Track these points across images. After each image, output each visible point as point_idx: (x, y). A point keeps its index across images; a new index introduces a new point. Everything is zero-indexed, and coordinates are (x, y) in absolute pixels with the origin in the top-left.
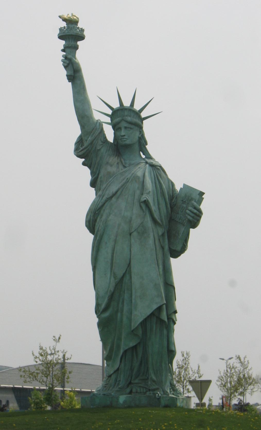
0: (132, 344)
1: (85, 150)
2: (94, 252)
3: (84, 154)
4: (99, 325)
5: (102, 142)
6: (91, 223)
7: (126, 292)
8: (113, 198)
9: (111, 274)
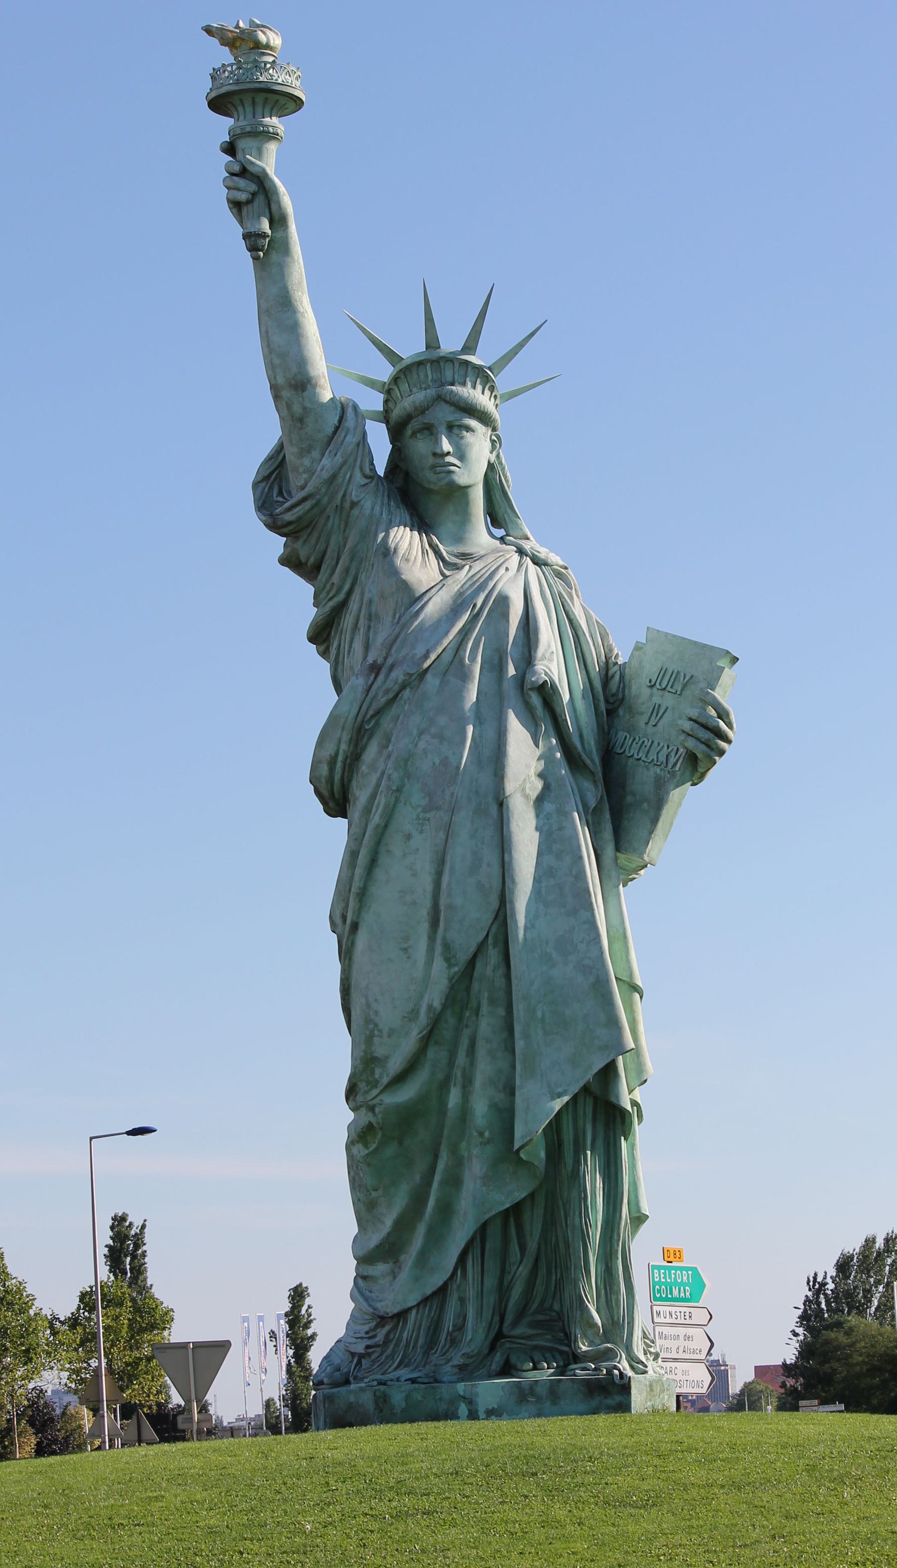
0: (502, 1200)
1: (307, 505)
2: (358, 871)
3: (299, 519)
4: (360, 1136)
5: (366, 477)
6: (339, 765)
7: (485, 1009)
8: (429, 676)
9: (431, 950)
